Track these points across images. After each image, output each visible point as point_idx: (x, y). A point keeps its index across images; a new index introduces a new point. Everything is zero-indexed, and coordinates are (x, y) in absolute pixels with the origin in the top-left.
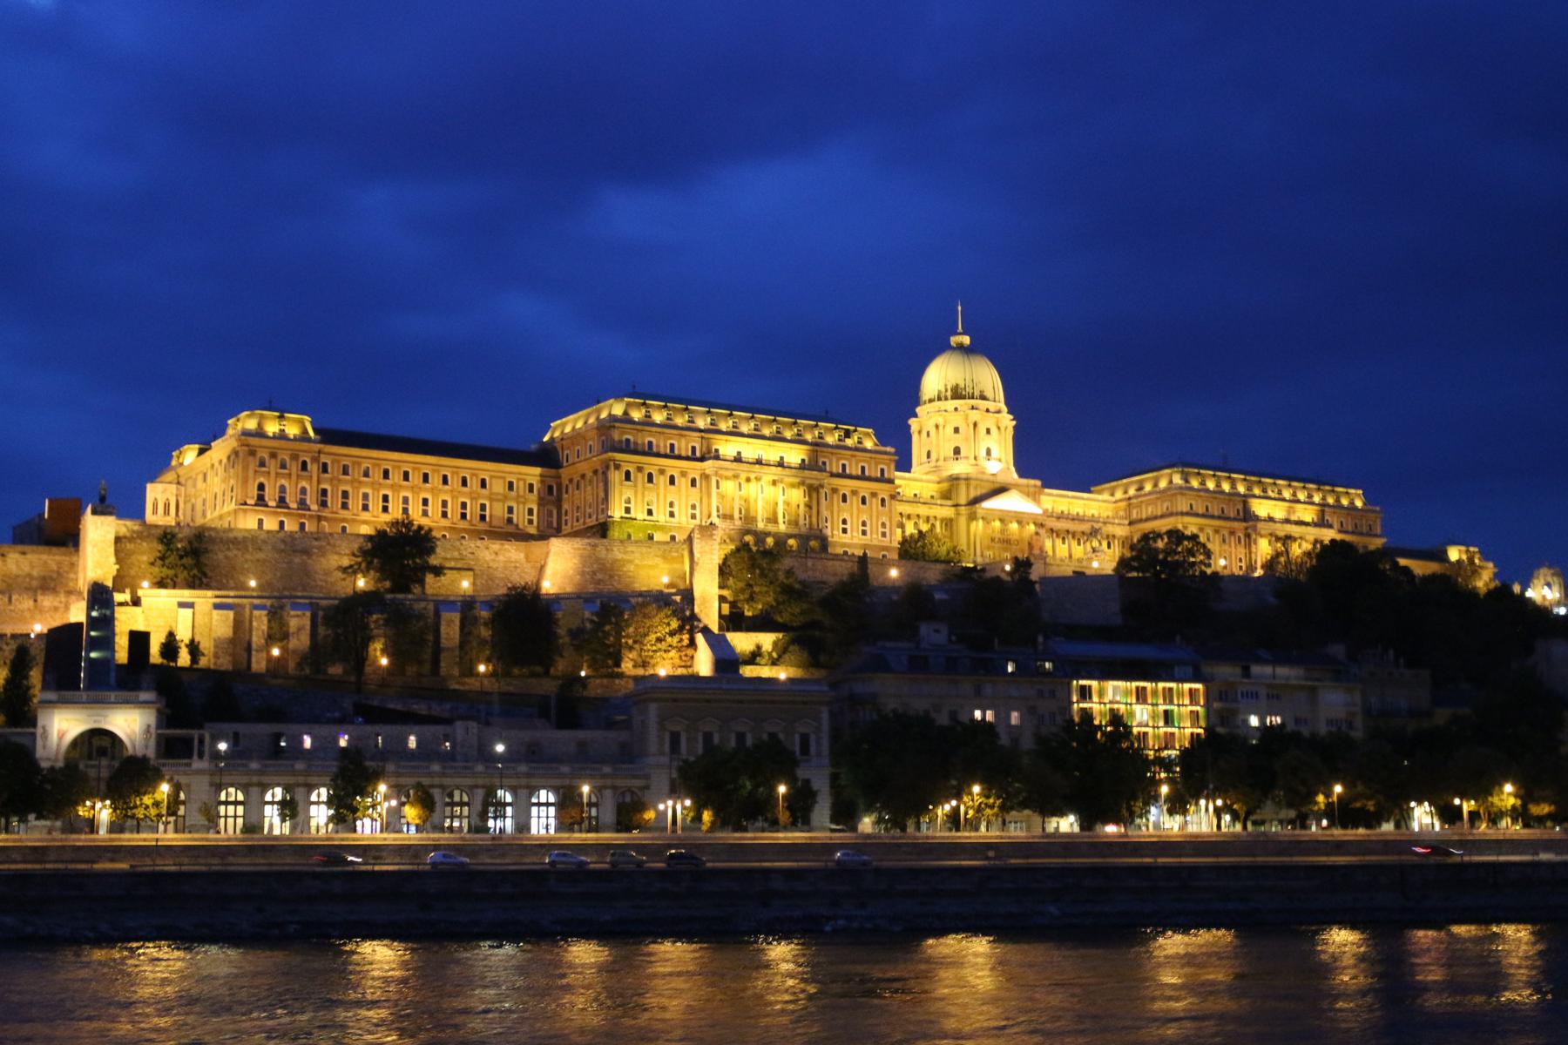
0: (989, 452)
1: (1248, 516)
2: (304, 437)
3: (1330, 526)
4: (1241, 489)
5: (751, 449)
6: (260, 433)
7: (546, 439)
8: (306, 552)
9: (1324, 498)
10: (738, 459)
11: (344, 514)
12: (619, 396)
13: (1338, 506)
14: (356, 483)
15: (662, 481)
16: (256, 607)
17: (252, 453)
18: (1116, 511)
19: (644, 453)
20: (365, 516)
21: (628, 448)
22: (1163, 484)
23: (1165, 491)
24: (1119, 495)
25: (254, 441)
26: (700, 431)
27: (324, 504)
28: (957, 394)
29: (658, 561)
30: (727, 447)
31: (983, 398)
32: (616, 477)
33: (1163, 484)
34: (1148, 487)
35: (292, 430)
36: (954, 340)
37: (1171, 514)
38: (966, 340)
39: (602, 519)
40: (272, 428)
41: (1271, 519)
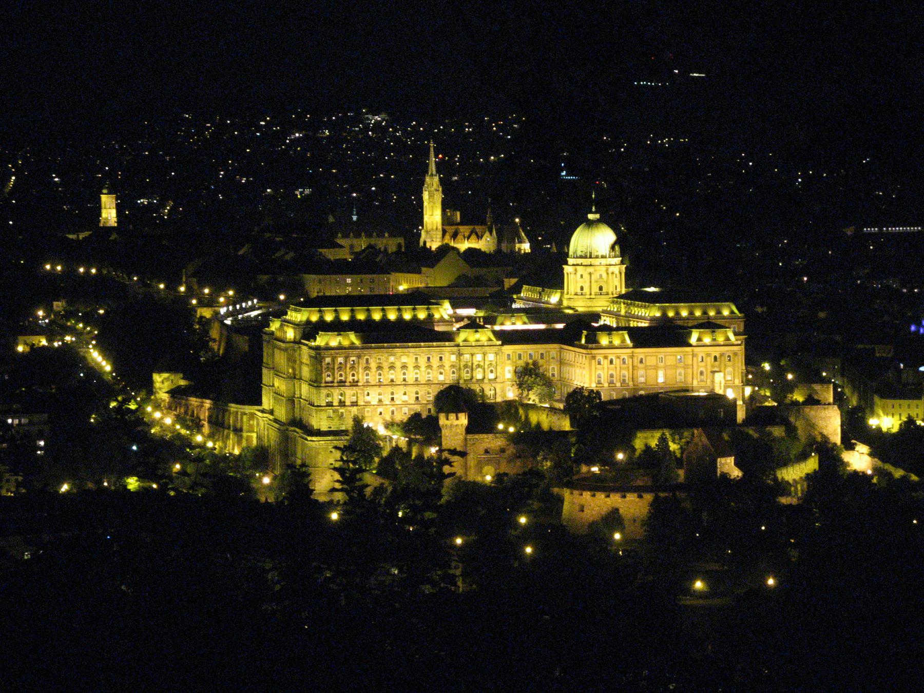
36: (590, 216)
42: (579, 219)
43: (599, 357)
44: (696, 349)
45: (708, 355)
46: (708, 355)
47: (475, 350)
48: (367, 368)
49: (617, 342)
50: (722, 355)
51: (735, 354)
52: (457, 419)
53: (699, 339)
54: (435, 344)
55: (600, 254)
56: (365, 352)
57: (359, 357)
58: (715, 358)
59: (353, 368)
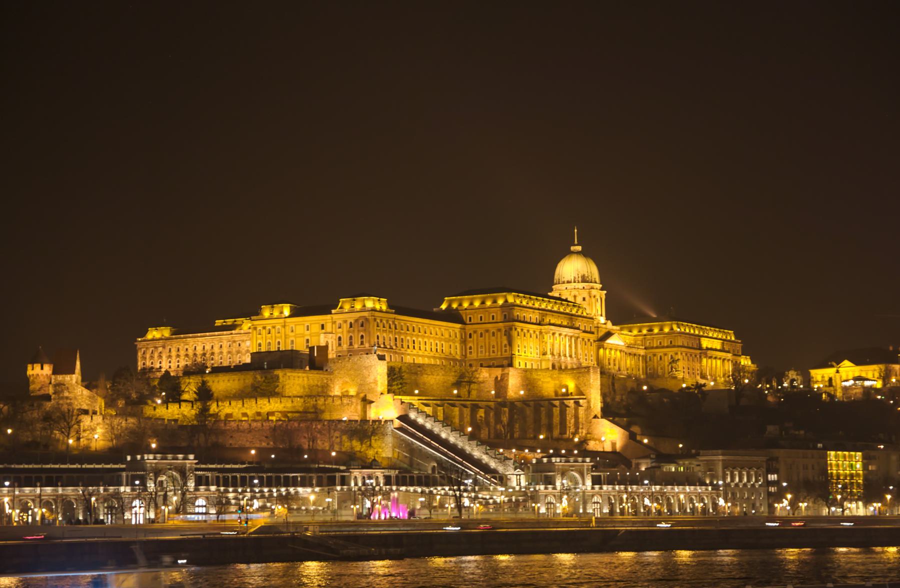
1: (700, 348)
3: (728, 352)
4: (697, 332)
6: (374, 310)
7: (444, 306)
8: (416, 374)
12: (510, 291)
16: (438, 405)
17: (375, 320)
18: (635, 341)
20: (409, 351)
22: (666, 330)
23: (668, 333)
24: (635, 332)
25: (377, 314)
26: (539, 309)
27: (396, 345)
28: (584, 280)
29: (549, 379)
32: (514, 333)
33: (666, 330)
34: (656, 331)
36: (572, 248)
37: (674, 346)
38: (579, 248)
39: (507, 354)
41: (711, 349)
42: (566, 253)
43: (259, 328)
44: (335, 317)
45: (345, 322)
46: (345, 322)
47: (245, 338)
48: (170, 357)
49: (276, 313)
50: (356, 321)
51: (367, 319)
52: (42, 369)
53: (341, 308)
54: (216, 333)
55: (566, 280)
56: (168, 342)
57: (164, 347)
58: (351, 324)
59: (160, 357)
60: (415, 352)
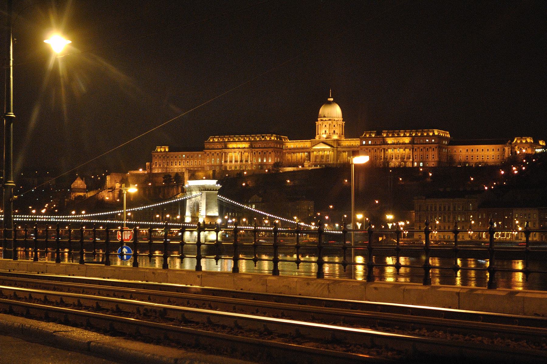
0: (325, 132)
2: (165, 151)
5: (234, 145)
9: (416, 134)
10: (234, 148)
11: (172, 167)
13: (422, 135)
14: (174, 160)
15: (215, 155)
19: (212, 149)
20: (176, 166)
21: (208, 149)
30: (230, 146)
31: (324, 117)
35: (163, 150)
38: (332, 99)
40: (159, 150)
60: (180, 166)
